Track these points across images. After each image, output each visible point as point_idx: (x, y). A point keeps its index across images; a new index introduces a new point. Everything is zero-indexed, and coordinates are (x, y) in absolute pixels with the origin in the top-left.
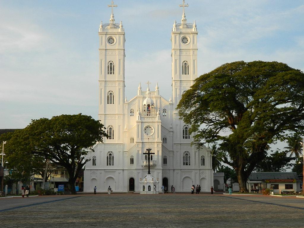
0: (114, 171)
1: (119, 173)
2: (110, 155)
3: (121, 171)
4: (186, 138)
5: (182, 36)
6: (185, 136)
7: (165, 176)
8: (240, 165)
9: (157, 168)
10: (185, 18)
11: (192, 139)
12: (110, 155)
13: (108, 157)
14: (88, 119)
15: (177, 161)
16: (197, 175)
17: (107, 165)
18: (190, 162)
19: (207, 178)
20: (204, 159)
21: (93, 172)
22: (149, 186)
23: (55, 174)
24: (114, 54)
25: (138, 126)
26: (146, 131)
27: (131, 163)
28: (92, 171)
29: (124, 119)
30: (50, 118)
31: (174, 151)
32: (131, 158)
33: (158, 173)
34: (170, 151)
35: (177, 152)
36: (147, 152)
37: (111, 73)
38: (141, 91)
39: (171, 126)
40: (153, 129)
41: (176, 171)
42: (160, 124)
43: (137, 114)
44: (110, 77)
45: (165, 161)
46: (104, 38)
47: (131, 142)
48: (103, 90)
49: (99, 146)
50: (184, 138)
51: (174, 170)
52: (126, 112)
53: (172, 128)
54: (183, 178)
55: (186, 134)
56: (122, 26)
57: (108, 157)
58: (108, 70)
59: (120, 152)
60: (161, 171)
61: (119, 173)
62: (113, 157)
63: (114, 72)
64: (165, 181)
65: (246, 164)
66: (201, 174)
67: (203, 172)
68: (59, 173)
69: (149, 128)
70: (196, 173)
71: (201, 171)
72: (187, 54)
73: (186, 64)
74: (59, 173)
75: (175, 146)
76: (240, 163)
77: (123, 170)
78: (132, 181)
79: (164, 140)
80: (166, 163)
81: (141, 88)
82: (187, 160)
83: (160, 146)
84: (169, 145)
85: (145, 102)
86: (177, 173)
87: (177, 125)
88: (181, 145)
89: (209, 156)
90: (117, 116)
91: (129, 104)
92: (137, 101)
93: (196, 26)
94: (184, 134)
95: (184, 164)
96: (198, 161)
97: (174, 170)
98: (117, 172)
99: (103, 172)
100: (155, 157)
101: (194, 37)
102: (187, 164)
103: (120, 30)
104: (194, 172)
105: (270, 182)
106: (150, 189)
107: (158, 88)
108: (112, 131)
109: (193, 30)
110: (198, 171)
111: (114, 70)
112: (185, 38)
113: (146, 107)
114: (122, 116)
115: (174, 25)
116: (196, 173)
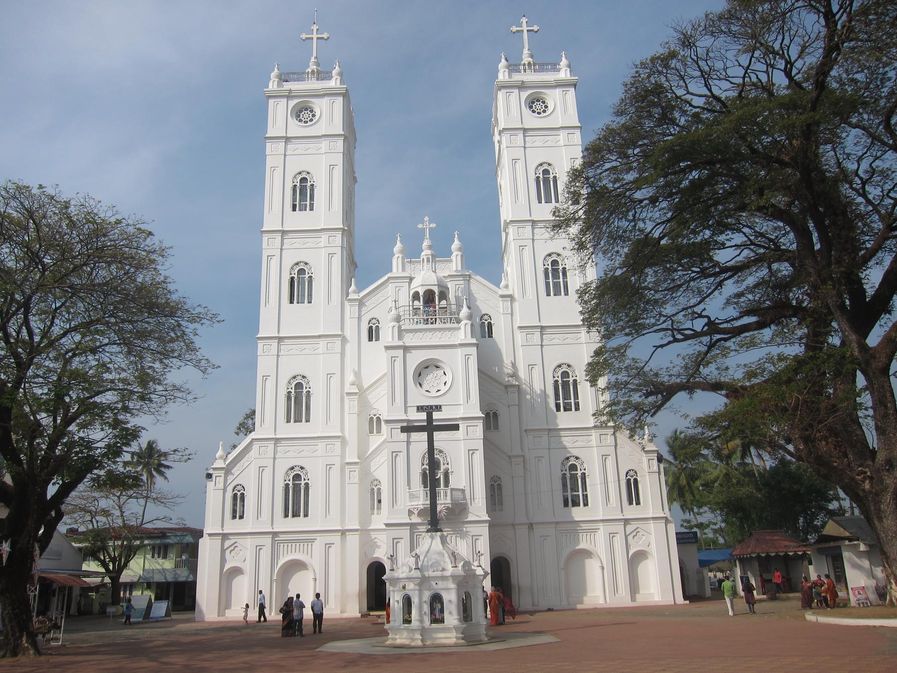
0: (306, 538)
2: (297, 477)
3: (336, 538)
5: (525, 94)
6: (561, 401)
10: (530, 60)
12: (297, 477)
13: (287, 485)
16: (619, 541)
19: (653, 550)
20: (636, 481)
21: (233, 541)
22: (436, 599)
25: (393, 359)
35: (539, 458)
47: (371, 432)
49: (256, 446)
51: (531, 526)
52: (350, 331)
55: (567, 396)
57: (287, 485)
58: (294, 200)
60: (484, 530)
61: (328, 546)
62: (307, 485)
64: (500, 568)
66: (630, 538)
67: (636, 531)
69: (432, 368)
73: (546, 172)
77: (343, 532)
78: (376, 575)
89: (655, 468)
90: (322, 343)
92: (391, 287)
96: (616, 491)
98: (321, 541)
100: (458, 480)
106: (442, 611)
111: (312, 198)
113: (419, 304)
114: (338, 342)
116: (612, 535)
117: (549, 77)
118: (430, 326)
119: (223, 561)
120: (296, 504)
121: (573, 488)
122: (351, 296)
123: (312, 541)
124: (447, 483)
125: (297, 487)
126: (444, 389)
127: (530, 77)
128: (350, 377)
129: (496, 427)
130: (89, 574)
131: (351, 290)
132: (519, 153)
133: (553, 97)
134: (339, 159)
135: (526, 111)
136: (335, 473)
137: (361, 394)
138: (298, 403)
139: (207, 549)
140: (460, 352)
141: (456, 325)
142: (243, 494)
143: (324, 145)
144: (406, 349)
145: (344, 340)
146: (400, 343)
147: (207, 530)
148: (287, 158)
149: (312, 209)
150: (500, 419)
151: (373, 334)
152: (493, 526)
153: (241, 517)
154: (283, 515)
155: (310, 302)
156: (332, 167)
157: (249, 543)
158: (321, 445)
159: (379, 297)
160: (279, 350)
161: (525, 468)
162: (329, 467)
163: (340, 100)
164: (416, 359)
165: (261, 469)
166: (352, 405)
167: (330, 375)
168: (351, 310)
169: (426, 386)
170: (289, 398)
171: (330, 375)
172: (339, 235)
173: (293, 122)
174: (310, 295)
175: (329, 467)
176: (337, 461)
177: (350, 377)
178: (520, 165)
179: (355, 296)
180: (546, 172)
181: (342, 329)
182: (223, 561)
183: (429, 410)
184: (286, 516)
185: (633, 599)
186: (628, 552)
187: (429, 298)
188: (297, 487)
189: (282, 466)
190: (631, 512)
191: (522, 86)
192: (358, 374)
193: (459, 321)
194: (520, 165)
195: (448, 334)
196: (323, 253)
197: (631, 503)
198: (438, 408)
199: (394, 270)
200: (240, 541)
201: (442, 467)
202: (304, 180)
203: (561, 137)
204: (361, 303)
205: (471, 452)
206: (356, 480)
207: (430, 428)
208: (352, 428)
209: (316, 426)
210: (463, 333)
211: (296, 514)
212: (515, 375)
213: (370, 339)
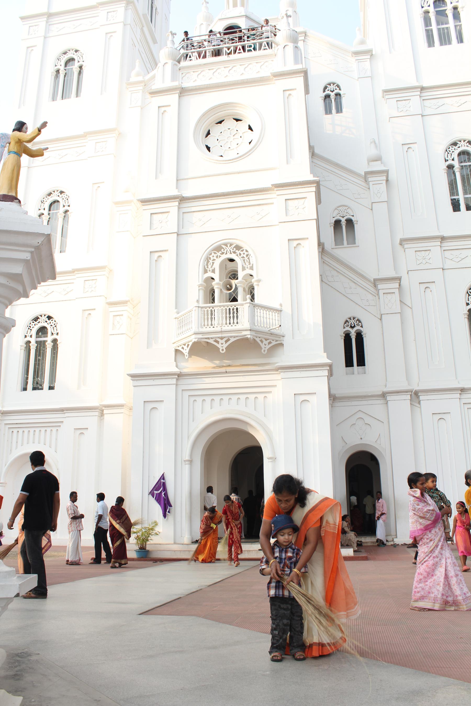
1: (81, 431)
9: (285, 357)
12: (42, 331)
17: (25, 389)
26: (210, 141)
33: (301, 398)
34: (375, 283)
35: (426, 285)
39: (373, 152)
41: (428, 404)
45: (354, 350)
53: (378, 159)
59: (88, 312)
61: (81, 431)
62: (55, 341)
77: (100, 411)
84: (369, 252)
86: (441, 416)
87: (408, 146)
97: (415, 396)
98: (71, 422)
120: (38, 372)
125: (41, 346)
131: (134, 73)
150: (357, 227)
154: (19, 386)
162: (88, 312)
164: (199, 105)
188: (41, 346)
211: (37, 387)
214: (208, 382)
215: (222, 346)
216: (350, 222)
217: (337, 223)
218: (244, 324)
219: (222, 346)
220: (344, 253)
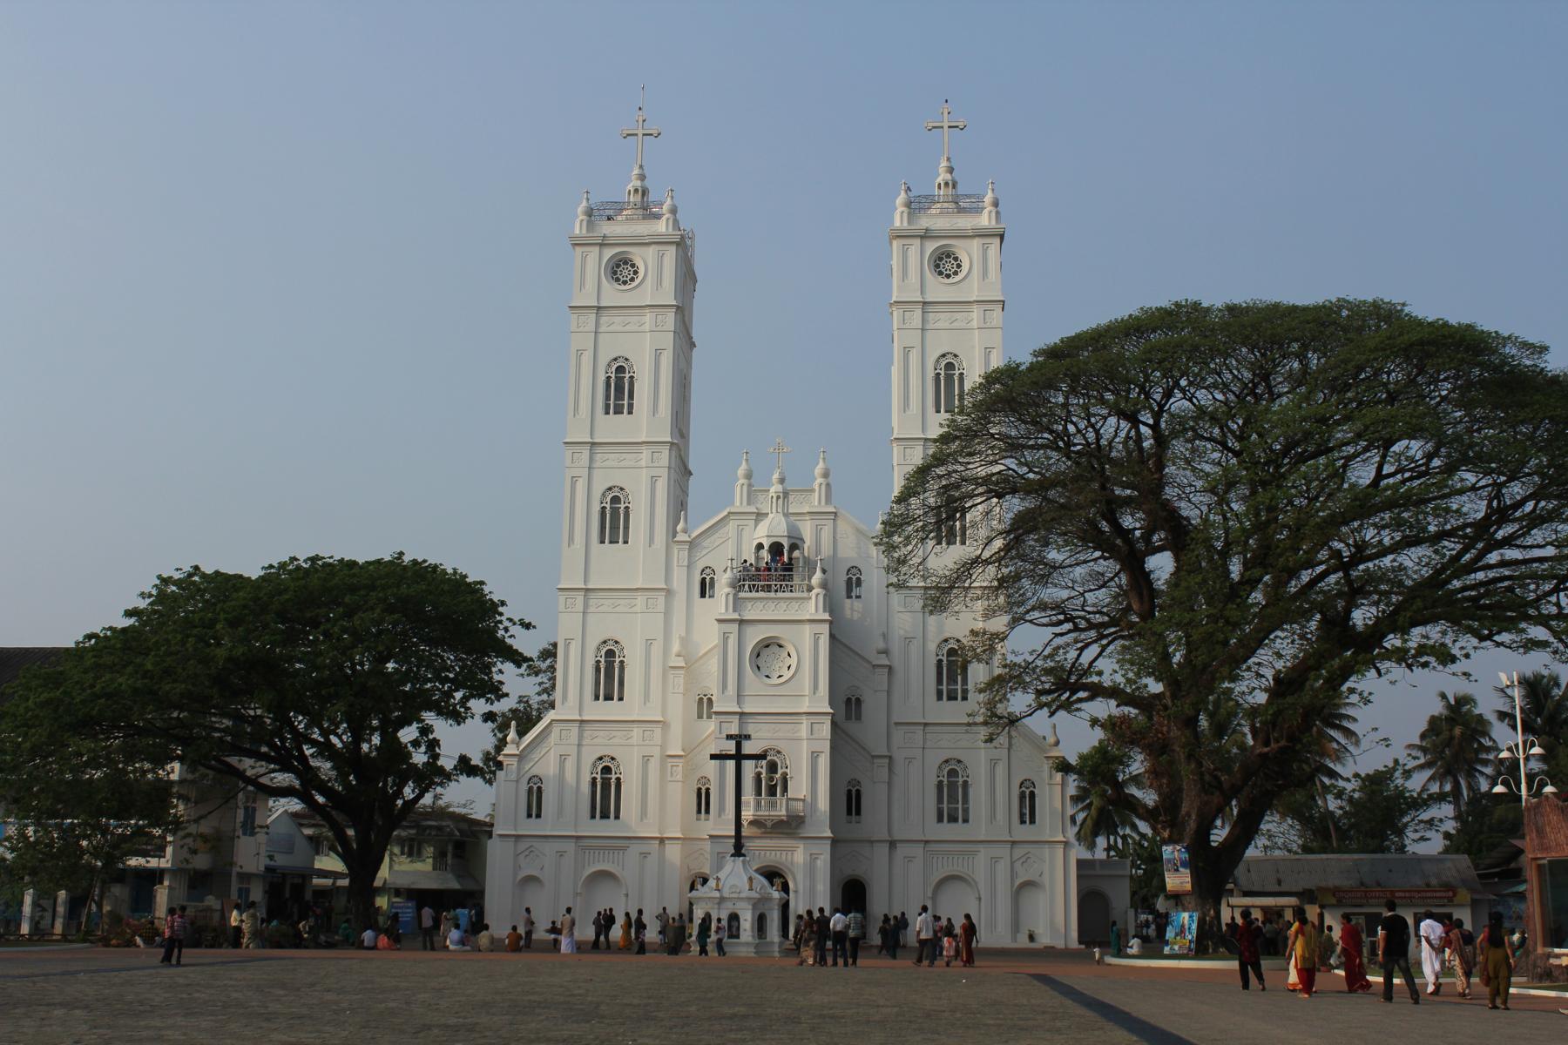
1: (645, 855)
2: (607, 770)
4: (952, 697)
5: (931, 246)
7: (850, 871)
8: (1188, 814)
9: (808, 831)
10: (948, 177)
11: (976, 700)
12: (607, 770)
13: (594, 779)
14: (423, 573)
15: (908, 804)
16: (1002, 869)
18: (966, 811)
20: (1032, 795)
23: (410, 854)
24: (635, 328)
27: (699, 811)
28: (523, 845)
29: (667, 613)
30: (254, 573)
31: (899, 756)
32: (699, 790)
35: (909, 760)
36: (730, 747)
37: (618, 411)
38: (750, 485)
39: (881, 645)
40: (794, 654)
41: (901, 851)
42: (825, 628)
43: (723, 588)
44: (613, 428)
46: (595, 261)
47: (700, 716)
48: (581, 485)
49: (556, 730)
50: (940, 697)
51: (893, 844)
52: (679, 580)
53: (886, 652)
54: (937, 877)
56: (674, 211)
57: (594, 779)
58: (608, 397)
60: (827, 847)
61: (645, 855)
62: (618, 779)
63: (631, 406)
65: (1207, 783)
66: (1018, 865)
68: (429, 850)
70: (994, 860)
71: (1019, 851)
72: (955, 325)
74: (429, 850)
75: (898, 735)
76: (1189, 806)
77: (662, 840)
79: (847, 707)
80: (858, 813)
81: (749, 476)
82: (953, 798)
83: (825, 729)
84: (872, 728)
85: (763, 533)
86: (910, 859)
88: (929, 729)
90: (640, 600)
91: (692, 545)
92: (732, 526)
93: (996, 204)
94: (939, 681)
95: (940, 819)
98: (635, 849)
99: (570, 846)
100: (799, 787)
101: (985, 251)
102: (953, 819)
103: (662, 227)
104: (983, 855)
105: (1340, 904)
107: (826, 475)
108: (617, 665)
109: (985, 220)
110: (1004, 851)
111: (631, 396)
112: (948, 256)
115: (901, 198)
116: (994, 860)
117: (965, 222)
118: (772, 595)
119: (517, 867)
121: (952, 796)
122: (681, 537)
123: (625, 848)
124: (785, 789)
126: (787, 675)
127: (934, 220)
128: (676, 647)
129: (859, 718)
130: (324, 874)
131: (679, 528)
132: (914, 339)
133: (968, 253)
134: (667, 341)
135: (929, 275)
136: (654, 765)
137: (690, 665)
138: (609, 676)
139: (497, 855)
140: (807, 630)
141: (805, 595)
142: (539, 789)
143: (648, 318)
144: (741, 622)
145: (669, 592)
146: (736, 616)
147: (497, 831)
148: (601, 337)
149: (630, 412)
150: (864, 706)
151: (705, 588)
152: (835, 842)
153: (538, 816)
155: (626, 542)
156: (658, 353)
157: (549, 848)
158: (636, 732)
159: (716, 539)
160: (586, 605)
161: (890, 770)
162: (646, 759)
163: (671, 252)
164: (754, 636)
165: (563, 758)
166: (678, 681)
167: (649, 643)
168: (680, 555)
169: (765, 671)
170: (598, 669)
171: (649, 643)
172: (666, 451)
173: (609, 287)
174: (626, 528)
175: (646, 759)
176: (656, 752)
177: (676, 647)
178: (914, 357)
179: (685, 537)
180: (950, 366)
181: (668, 578)
182: (517, 867)
183: (739, 739)
184: (593, 816)
185: (1014, 939)
186: (1027, 880)
187: (776, 549)
189: (589, 757)
190: (1023, 832)
191: (926, 235)
192: (685, 641)
193: (810, 589)
194: (914, 357)
195: (795, 605)
196: (644, 475)
197: (1023, 822)
198: (748, 737)
199: (737, 503)
200: (537, 844)
201: (780, 771)
202: (620, 369)
203: (975, 315)
204: (692, 545)
205: (814, 756)
206: (679, 777)
207: (739, 757)
208: (678, 710)
209: (631, 706)
210: (812, 606)
211: (605, 816)
212: (886, 652)
213: (703, 595)
214: (758, 843)
215: (769, 824)
216: (858, 701)
217: (849, 700)
218: (781, 812)
219: (769, 824)
220: (852, 727)
